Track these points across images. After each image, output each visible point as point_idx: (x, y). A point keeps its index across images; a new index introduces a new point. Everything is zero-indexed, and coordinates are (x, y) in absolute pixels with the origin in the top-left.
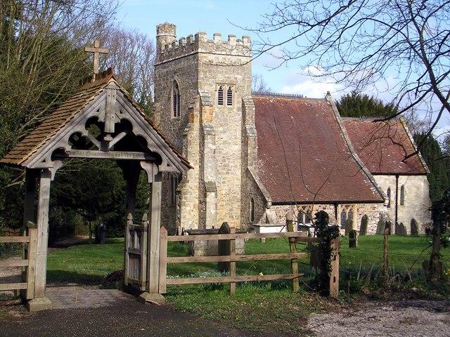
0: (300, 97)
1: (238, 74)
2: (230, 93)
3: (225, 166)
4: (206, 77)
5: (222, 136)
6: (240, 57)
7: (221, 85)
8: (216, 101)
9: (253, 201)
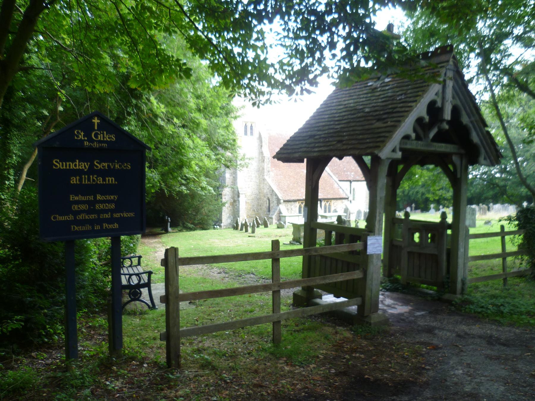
2: (251, 127)
9: (269, 200)
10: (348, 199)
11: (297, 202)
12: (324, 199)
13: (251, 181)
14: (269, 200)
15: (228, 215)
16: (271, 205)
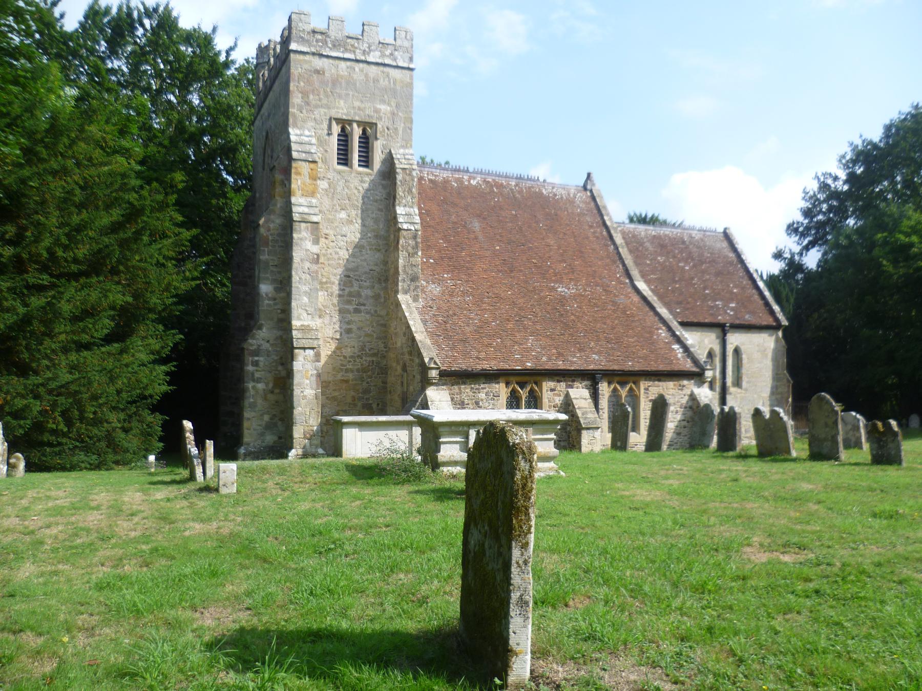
1: (383, 102)
5: (345, 229)
6: (387, 69)
7: (344, 124)
12: (610, 375)
13: (357, 311)
15: (266, 418)
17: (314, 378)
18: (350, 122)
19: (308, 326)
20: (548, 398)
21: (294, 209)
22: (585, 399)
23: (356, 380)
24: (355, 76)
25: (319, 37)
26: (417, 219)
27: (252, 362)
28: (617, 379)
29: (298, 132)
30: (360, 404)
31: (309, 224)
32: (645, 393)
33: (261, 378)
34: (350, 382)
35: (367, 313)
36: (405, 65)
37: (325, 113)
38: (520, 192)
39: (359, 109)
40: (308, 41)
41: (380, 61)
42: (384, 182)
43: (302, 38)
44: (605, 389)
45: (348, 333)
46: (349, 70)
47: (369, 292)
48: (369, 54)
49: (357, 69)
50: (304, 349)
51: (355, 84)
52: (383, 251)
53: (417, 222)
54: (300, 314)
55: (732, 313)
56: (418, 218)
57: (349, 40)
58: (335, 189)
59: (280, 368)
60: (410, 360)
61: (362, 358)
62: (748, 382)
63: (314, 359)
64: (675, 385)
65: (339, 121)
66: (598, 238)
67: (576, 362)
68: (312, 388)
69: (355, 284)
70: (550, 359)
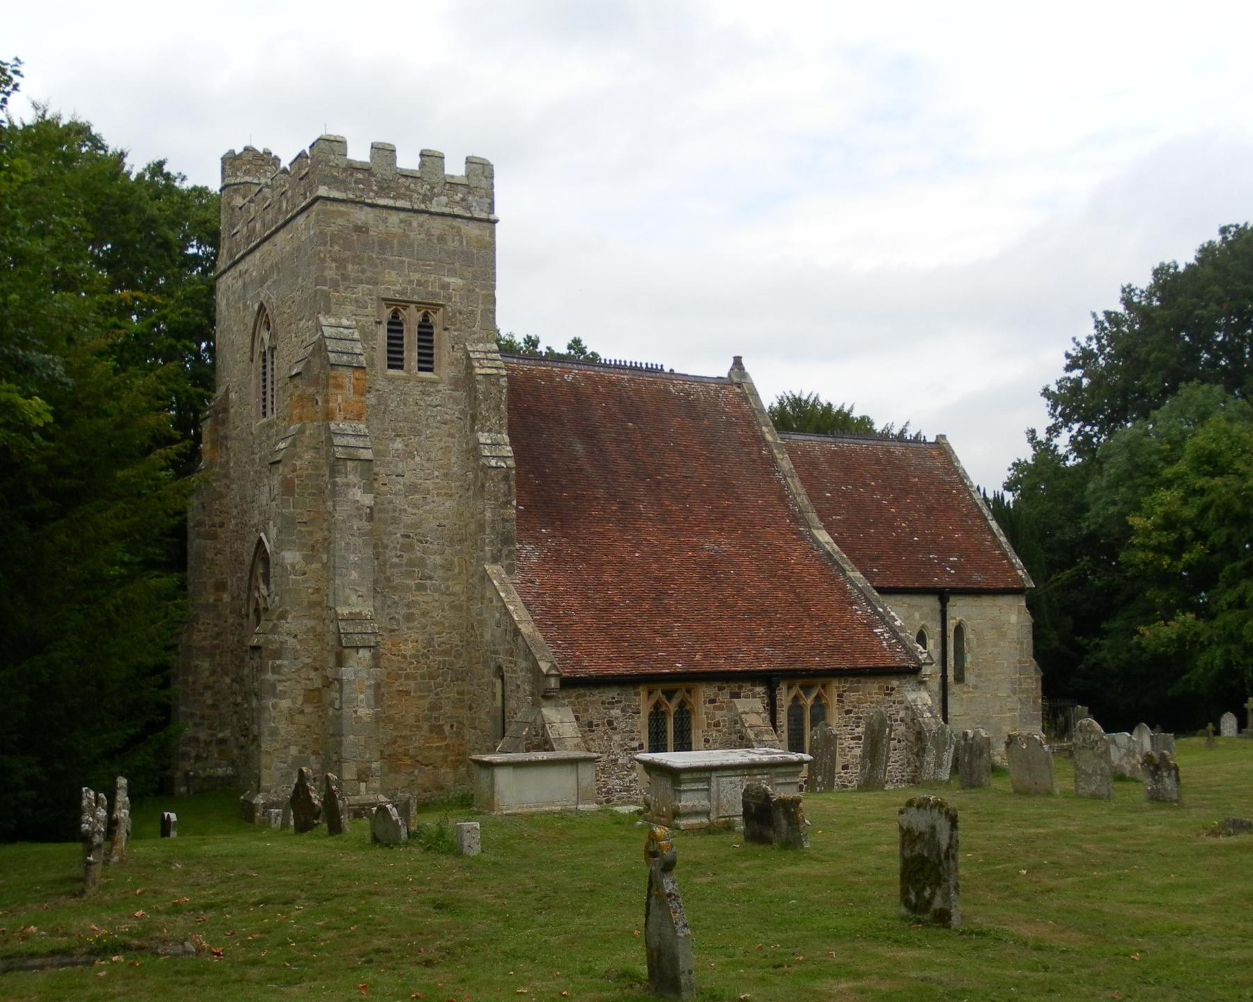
0: (654, 371)
1: (452, 272)
2: (425, 330)
3: (411, 563)
4: (345, 277)
6: (458, 222)
7: (396, 307)
8: (381, 355)
10: (915, 671)
11: (643, 691)
12: (791, 675)
14: (502, 678)
16: (512, 703)
17: (370, 692)
18: (406, 304)
19: (360, 613)
20: (706, 713)
21: (338, 441)
22: (758, 713)
23: (420, 691)
24: (412, 235)
25: (360, 176)
26: (508, 450)
27: (273, 668)
28: (799, 682)
29: (332, 321)
30: (426, 726)
31: (356, 462)
32: (838, 701)
33: (285, 692)
34: (412, 694)
35: (435, 590)
36: (484, 216)
37: (370, 290)
38: (636, 391)
39: (419, 283)
40: (343, 182)
41: (447, 210)
42: (456, 394)
43: (335, 177)
44: (784, 698)
45: (408, 622)
46: (402, 225)
47: (438, 559)
48: (431, 201)
49: (415, 224)
50: (357, 648)
51: (411, 246)
52: (457, 497)
53: (510, 454)
54: (347, 597)
55: (952, 572)
56: (509, 448)
57: (402, 180)
58: (387, 406)
59: (313, 674)
60: (511, 662)
61: (428, 658)
62: (979, 676)
63: (370, 663)
64: (880, 688)
65: (388, 301)
66: (754, 461)
67: (745, 661)
68: (369, 707)
69: (418, 547)
70: (705, 657)
